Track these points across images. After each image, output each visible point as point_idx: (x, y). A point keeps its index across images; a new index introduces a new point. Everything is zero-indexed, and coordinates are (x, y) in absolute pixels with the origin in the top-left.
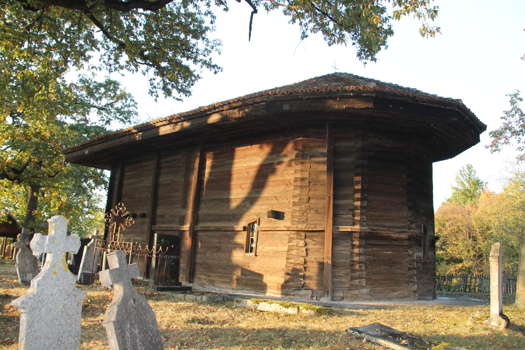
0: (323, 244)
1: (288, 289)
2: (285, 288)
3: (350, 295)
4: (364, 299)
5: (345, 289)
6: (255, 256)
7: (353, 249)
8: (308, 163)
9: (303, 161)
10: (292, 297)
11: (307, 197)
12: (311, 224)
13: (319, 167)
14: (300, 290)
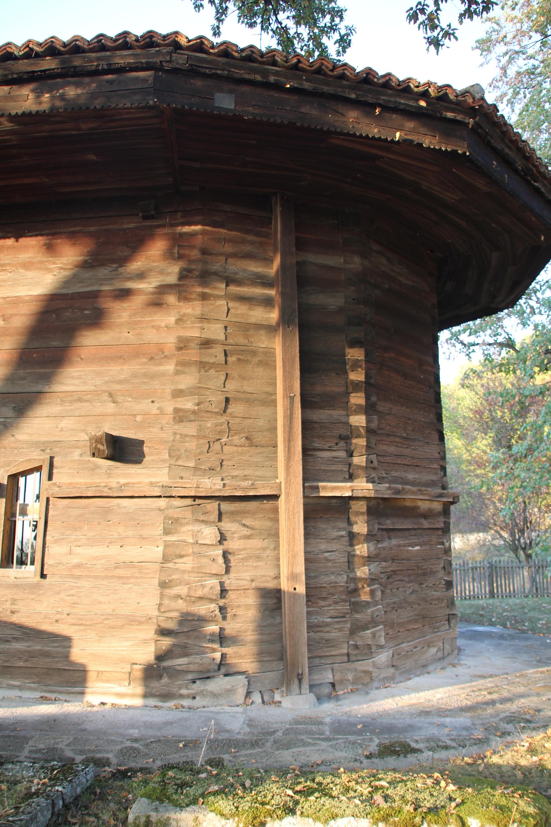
0: (275, 535)
1: (170, 677)
2: (161, 677)
3: (350, 677)
4: (384, 678)
5: (338, 659)
6: (38, 578)
7: (352, 545)
8: (219, 297)
9: (207, 290)
10: (186, 703)
11: (222, 398)
12: (233, 477)
13: (251, 313)
14: (208, 678)
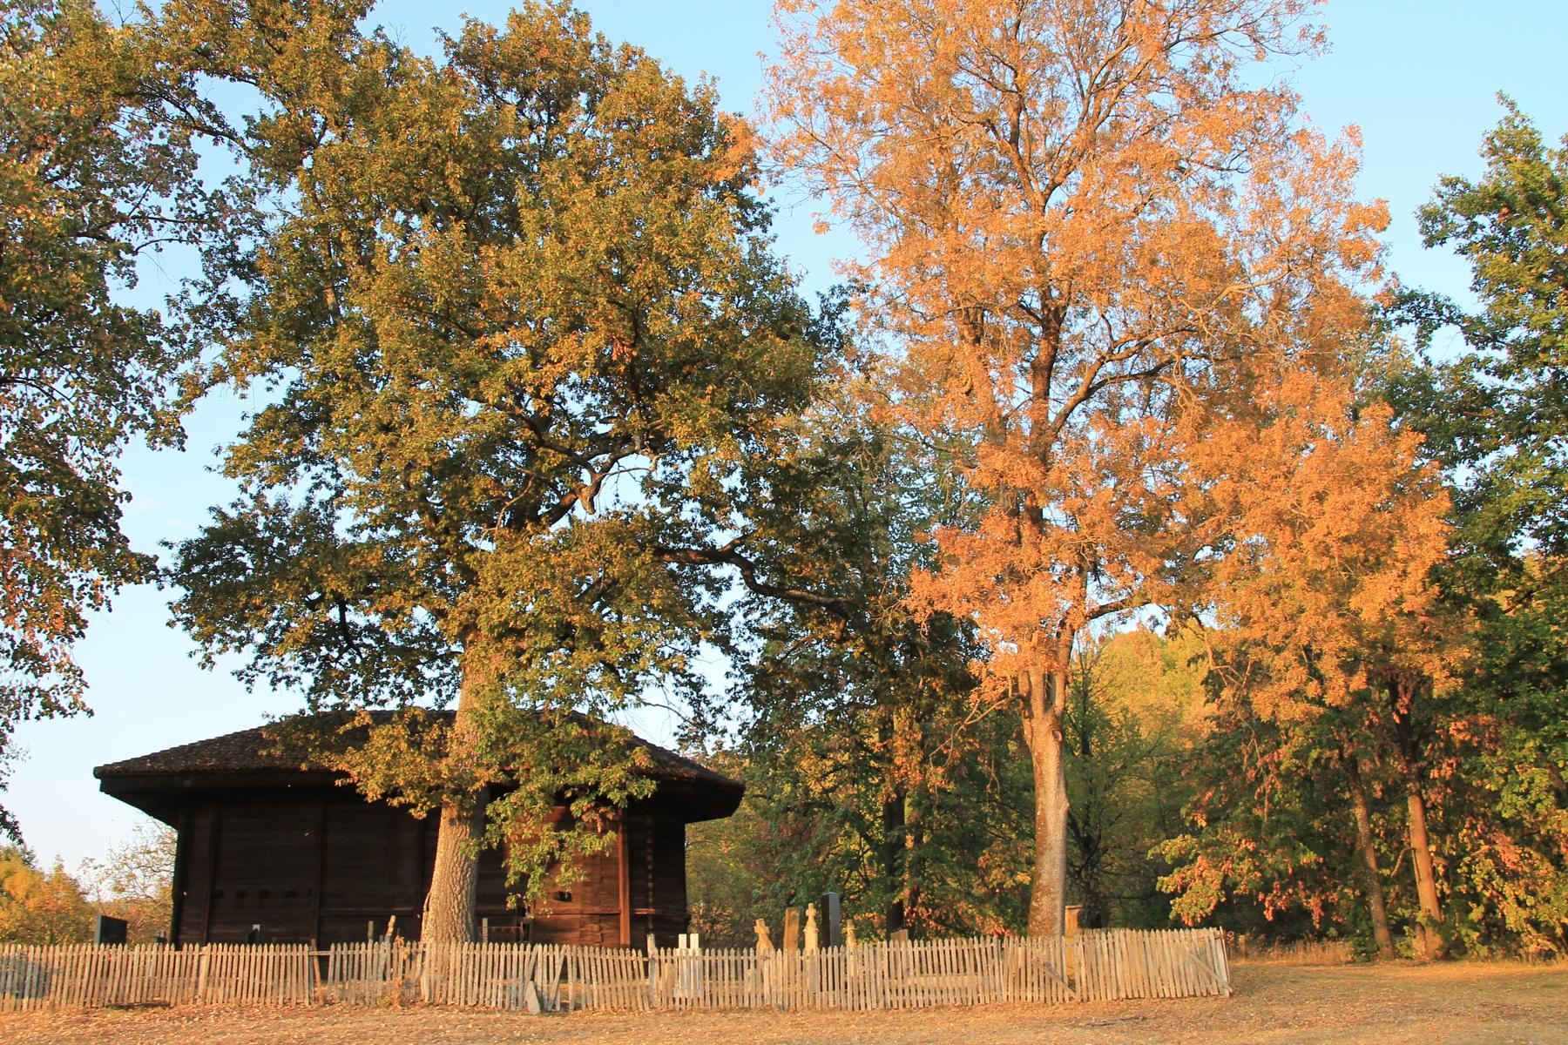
0: (618, 928)
